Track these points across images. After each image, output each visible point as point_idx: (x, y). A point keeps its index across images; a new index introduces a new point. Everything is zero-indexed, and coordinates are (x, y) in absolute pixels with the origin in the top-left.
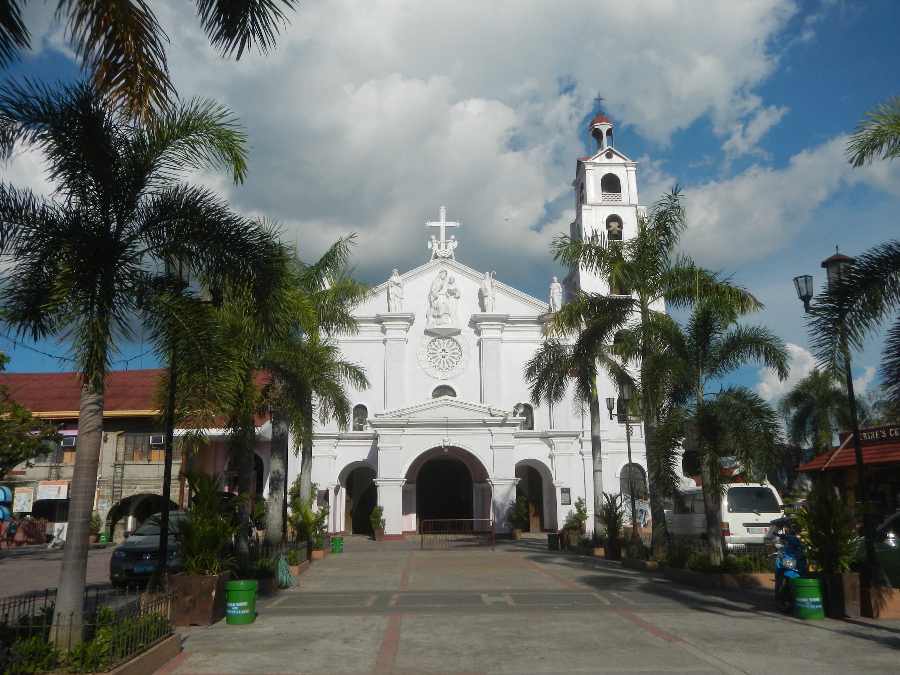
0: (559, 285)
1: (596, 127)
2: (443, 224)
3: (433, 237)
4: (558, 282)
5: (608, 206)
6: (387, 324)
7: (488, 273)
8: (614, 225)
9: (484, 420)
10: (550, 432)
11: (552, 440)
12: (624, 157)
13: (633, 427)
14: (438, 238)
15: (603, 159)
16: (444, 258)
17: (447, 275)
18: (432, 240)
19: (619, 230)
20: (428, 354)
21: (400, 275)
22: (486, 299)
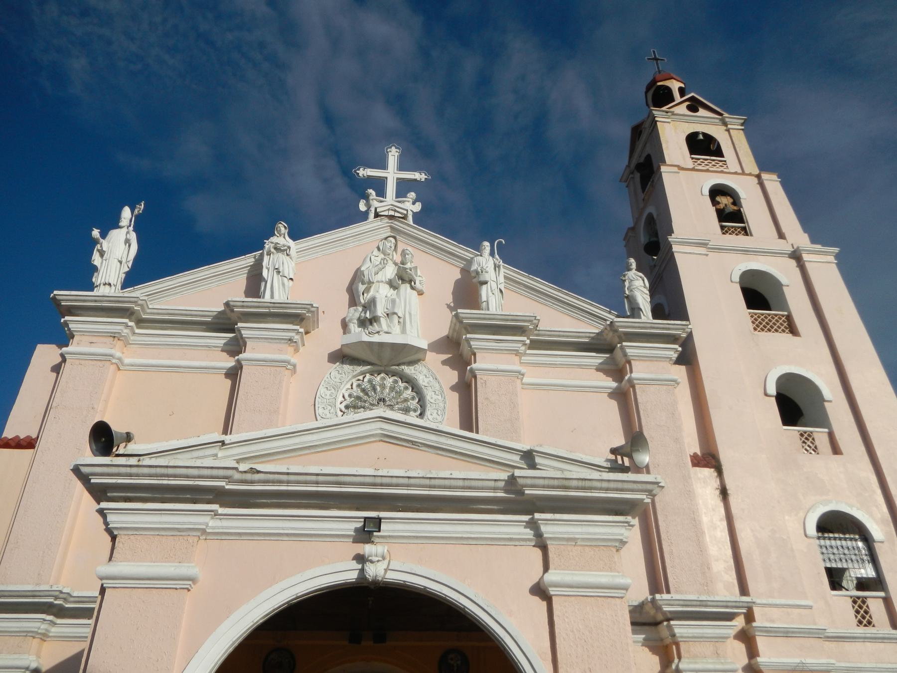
0: (641, 274)
1: (659, 84)
2: (392, 174)
3: (371, 192)
4: (638, 269)
5: (708, 171)
6: (247, 329)
7: (486, 244)
8: (724, 201)
9: (512, 479)
10: (670, 603)
11: (670, 627)
12: (719, 110)
13: (870, 602)
14: (381, 193)
15: (682, 109)
16: (391, 217)
17: (396, 246)
18: (366, 197)
19: (735, 208)
20: (342, 407)
21: (295, 235)
22: (484, 290)
